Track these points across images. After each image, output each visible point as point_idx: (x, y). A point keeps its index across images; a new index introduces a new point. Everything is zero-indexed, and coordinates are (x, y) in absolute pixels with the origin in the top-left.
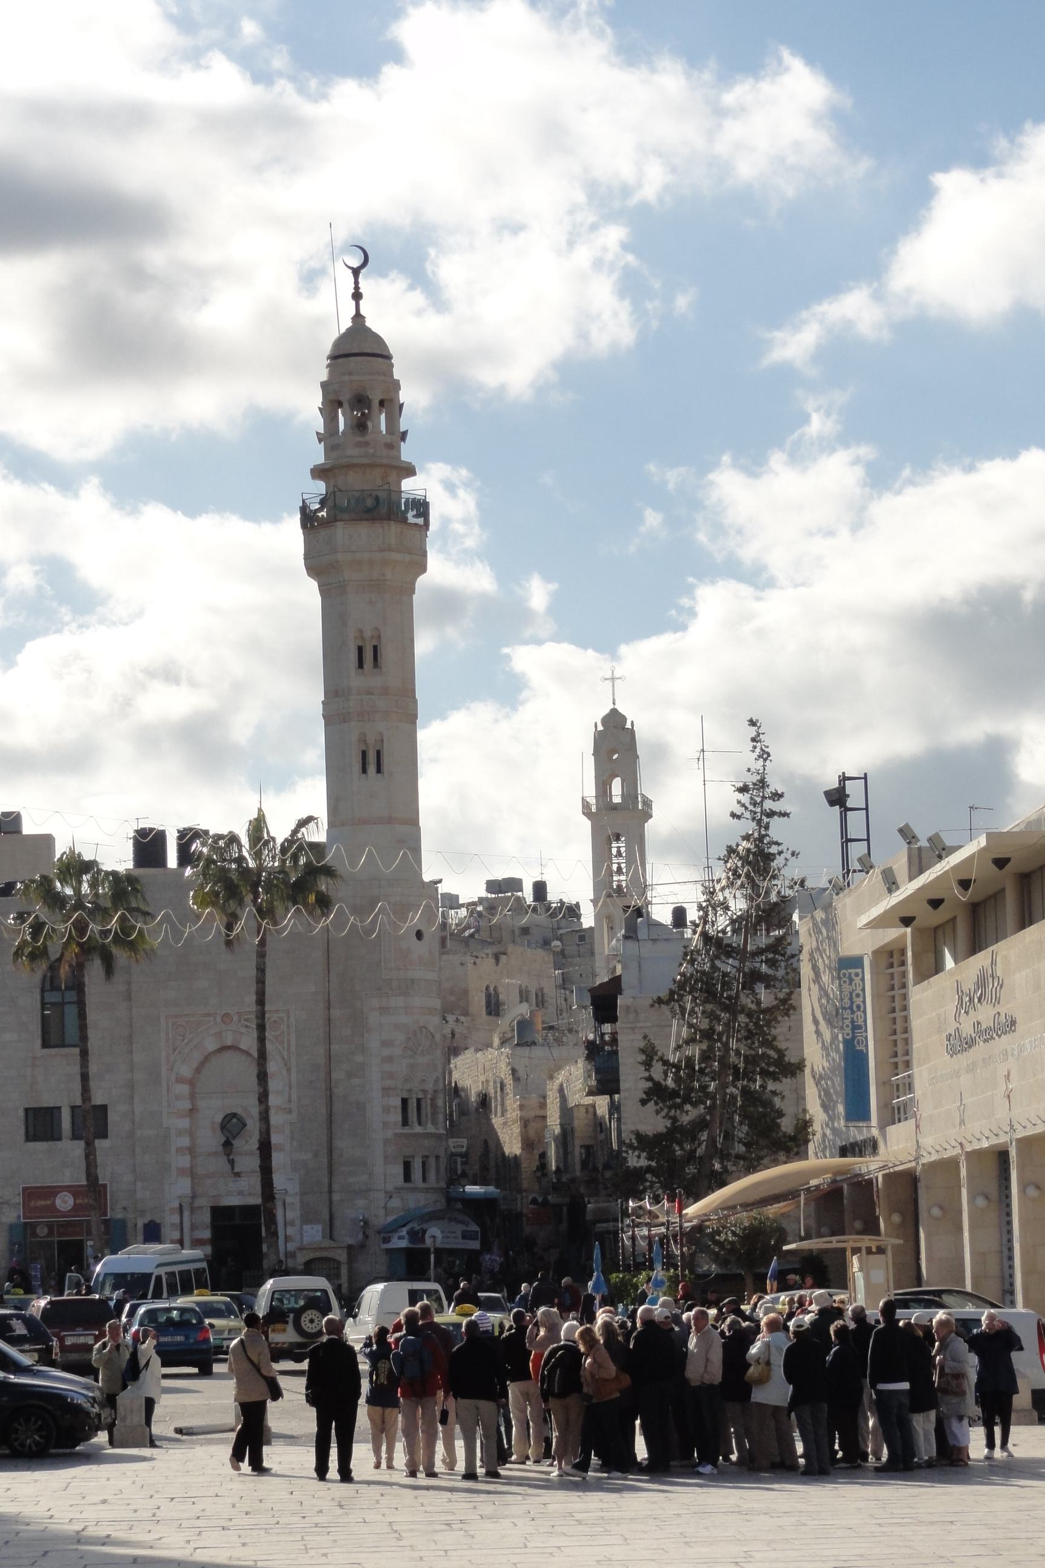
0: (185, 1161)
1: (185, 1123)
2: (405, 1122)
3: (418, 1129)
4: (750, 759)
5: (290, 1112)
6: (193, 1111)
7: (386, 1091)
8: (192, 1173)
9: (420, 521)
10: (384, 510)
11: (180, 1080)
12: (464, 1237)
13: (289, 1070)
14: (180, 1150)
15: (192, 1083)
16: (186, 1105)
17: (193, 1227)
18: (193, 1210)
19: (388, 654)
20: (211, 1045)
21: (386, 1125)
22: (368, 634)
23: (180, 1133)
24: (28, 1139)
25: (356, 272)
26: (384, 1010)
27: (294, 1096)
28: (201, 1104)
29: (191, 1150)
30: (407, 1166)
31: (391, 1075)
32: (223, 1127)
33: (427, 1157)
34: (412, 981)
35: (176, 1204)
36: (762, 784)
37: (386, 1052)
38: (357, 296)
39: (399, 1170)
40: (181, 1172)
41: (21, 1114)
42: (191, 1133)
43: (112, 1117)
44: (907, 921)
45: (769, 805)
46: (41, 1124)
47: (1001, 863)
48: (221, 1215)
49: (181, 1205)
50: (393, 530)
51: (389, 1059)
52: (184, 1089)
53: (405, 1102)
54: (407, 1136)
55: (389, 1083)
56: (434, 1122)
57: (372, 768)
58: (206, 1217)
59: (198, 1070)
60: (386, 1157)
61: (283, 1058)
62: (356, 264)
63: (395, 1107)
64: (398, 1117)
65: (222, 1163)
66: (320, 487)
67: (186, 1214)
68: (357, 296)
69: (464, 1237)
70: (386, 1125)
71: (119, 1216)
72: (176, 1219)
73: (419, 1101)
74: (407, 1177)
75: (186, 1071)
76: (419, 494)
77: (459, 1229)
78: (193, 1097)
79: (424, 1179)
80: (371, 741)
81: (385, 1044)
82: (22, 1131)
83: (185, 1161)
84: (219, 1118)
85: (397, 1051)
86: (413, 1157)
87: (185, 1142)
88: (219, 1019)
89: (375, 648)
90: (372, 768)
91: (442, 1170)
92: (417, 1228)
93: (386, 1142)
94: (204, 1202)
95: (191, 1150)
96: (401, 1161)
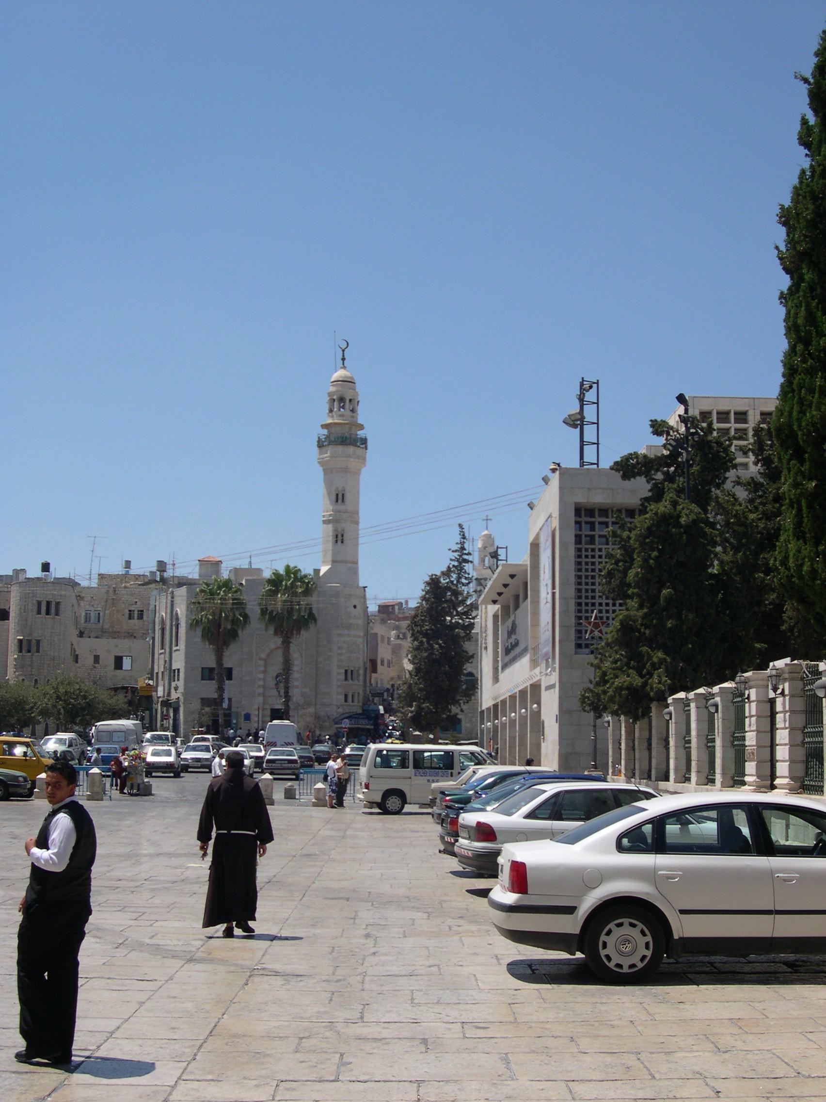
0: (261, 690)
1: (261, 676)
2: (346, 679)
4: (458, 538)
6: (265, 672)
7: (339, 667)
8: (264, 695)
9: (363, 446)
10: (348, 441)
11: (260, 659)
14: (259, 686)
15: (265, 660)
16: (262, 669)
17: (263, 716)
18: (263, 709)
19: (348, 497)
20: (273, 646)
21: (338, 680)
22: (340, 489)
23: (260, 679)
24: (202, 679)
25: (343, 351)
26: (340, 635)
29: (264, 687)
30: (346, 696)
32: (277, 677)
35: (256, 707)
36: (463, 548)
38: (343, 359)
39: (343, 697)
40: (259, 694)
41: (200, 669)
42: (264, 680)
43: (234, 672)
44: (495, 602)
45: (465, 557)
46: (208, 674)
47: (512, 576)
50: (351, 449)
51: (340, 654)
52: (262, 663)
53: (346, 671)
56: (358, 680)
57: (339, 542)
62: (344, 347)
64: (343, 677)
65: (275, 692)
66: (325, 432)
68: (343, 359)
70: (338, 680)
72: (257, 713)
74: (346, 701)
75: (263, 656)
76: (363, 436)
78: (265, 666)
80: (340, 530)
81: (340, 648)
82: (200, 676)
83: (261, 690)
84: (275, 675)
87: (261, 683)
90: (339, 542)
91: (361, 699)
93: (338, 686)
95: (264, 687)
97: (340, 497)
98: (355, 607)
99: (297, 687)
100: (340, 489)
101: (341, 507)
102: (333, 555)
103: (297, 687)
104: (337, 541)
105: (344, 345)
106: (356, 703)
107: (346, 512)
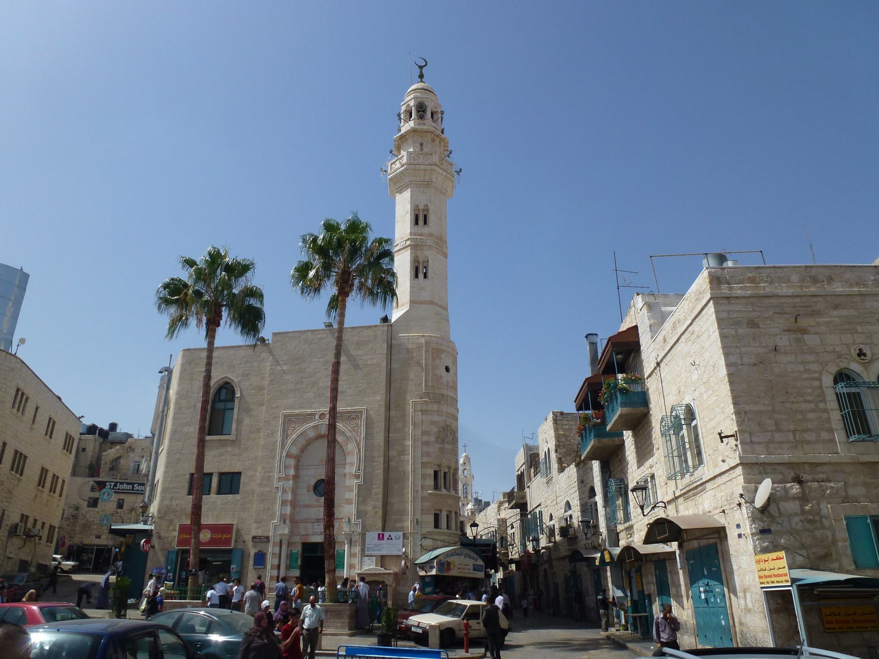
2: (436, 487)
3: (444, 491)
5: (358, 477)
12: (474, 569)
13: (359, 449)
15: (298, 459)
18: (289, 544)
19: (432, 218)
22: (421, 207)
25: (421, 67)
27: (362, 467)
28: (302, 473)
30: (437, 517)
31: (428, 454)
33: (450, 512)
34: (443, 395)
37: (425, 438)
39: (431, 518)
42: (294, 492)
48: (308, 547)
49: (281, 541)
51: (427, 443)
52: (292, 462)
53: (436, 473)
54: (436, 495)
55: (425, 459)
57: (421, 276)
58: (298, 549)
59: (302, 451)
60: (422, 510)
61: (356, 441)
63: (429, 475)
64: (431, 482)
67: (284, 547)
69: (474, 569)
71: (240, 547)
72: (277, 550)
73: (445, 473)
74: (437, 525)
77: (471, 562)
78: (297, 468)
79: (448, 528)
80: (421, 260)
85: (432, 439)
86: (441, 511)
88: (317, 417)
89: (425, 217)
92: (444, 560)
94: (298, 539)
96: (433, 512)
97: (421, 222)
98: (447, 369)
99: (349, 502)
100: (421, 207)
101: (421, 229)
102: (412, 292)
103: (349, 502)
104: (417, 276)
105: (423, 63)
106: (453, 531)
107: (431, 235)
